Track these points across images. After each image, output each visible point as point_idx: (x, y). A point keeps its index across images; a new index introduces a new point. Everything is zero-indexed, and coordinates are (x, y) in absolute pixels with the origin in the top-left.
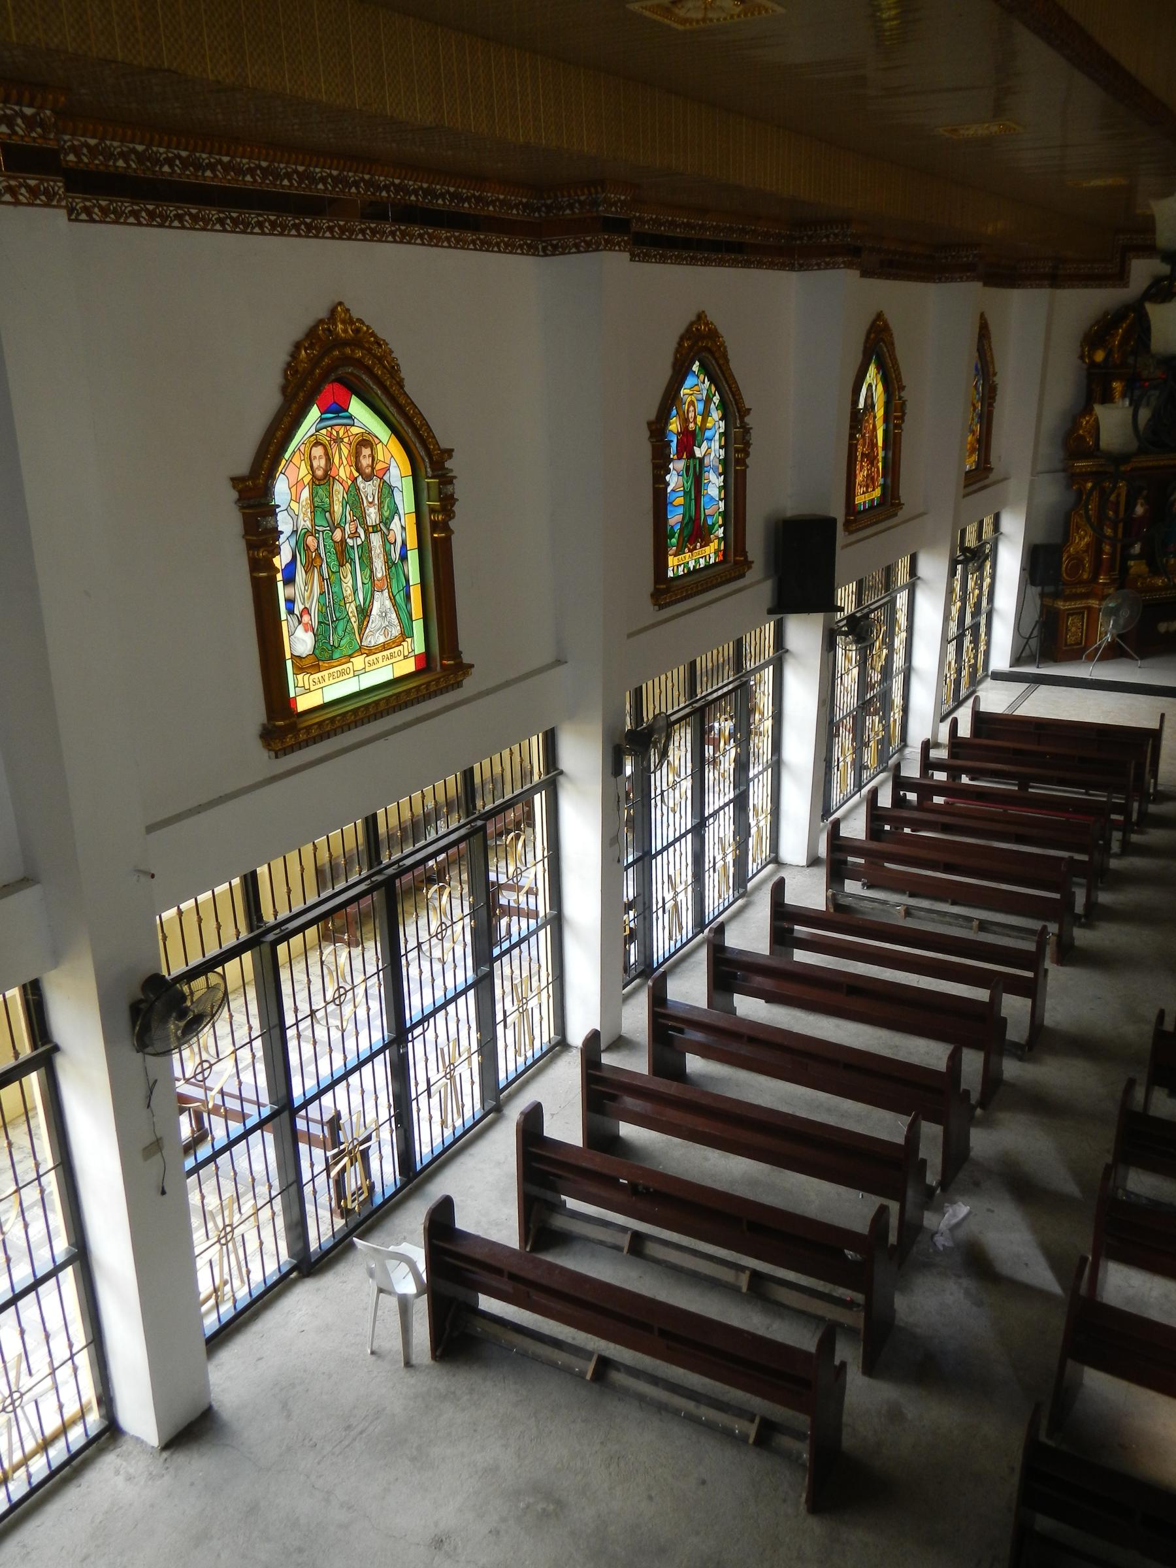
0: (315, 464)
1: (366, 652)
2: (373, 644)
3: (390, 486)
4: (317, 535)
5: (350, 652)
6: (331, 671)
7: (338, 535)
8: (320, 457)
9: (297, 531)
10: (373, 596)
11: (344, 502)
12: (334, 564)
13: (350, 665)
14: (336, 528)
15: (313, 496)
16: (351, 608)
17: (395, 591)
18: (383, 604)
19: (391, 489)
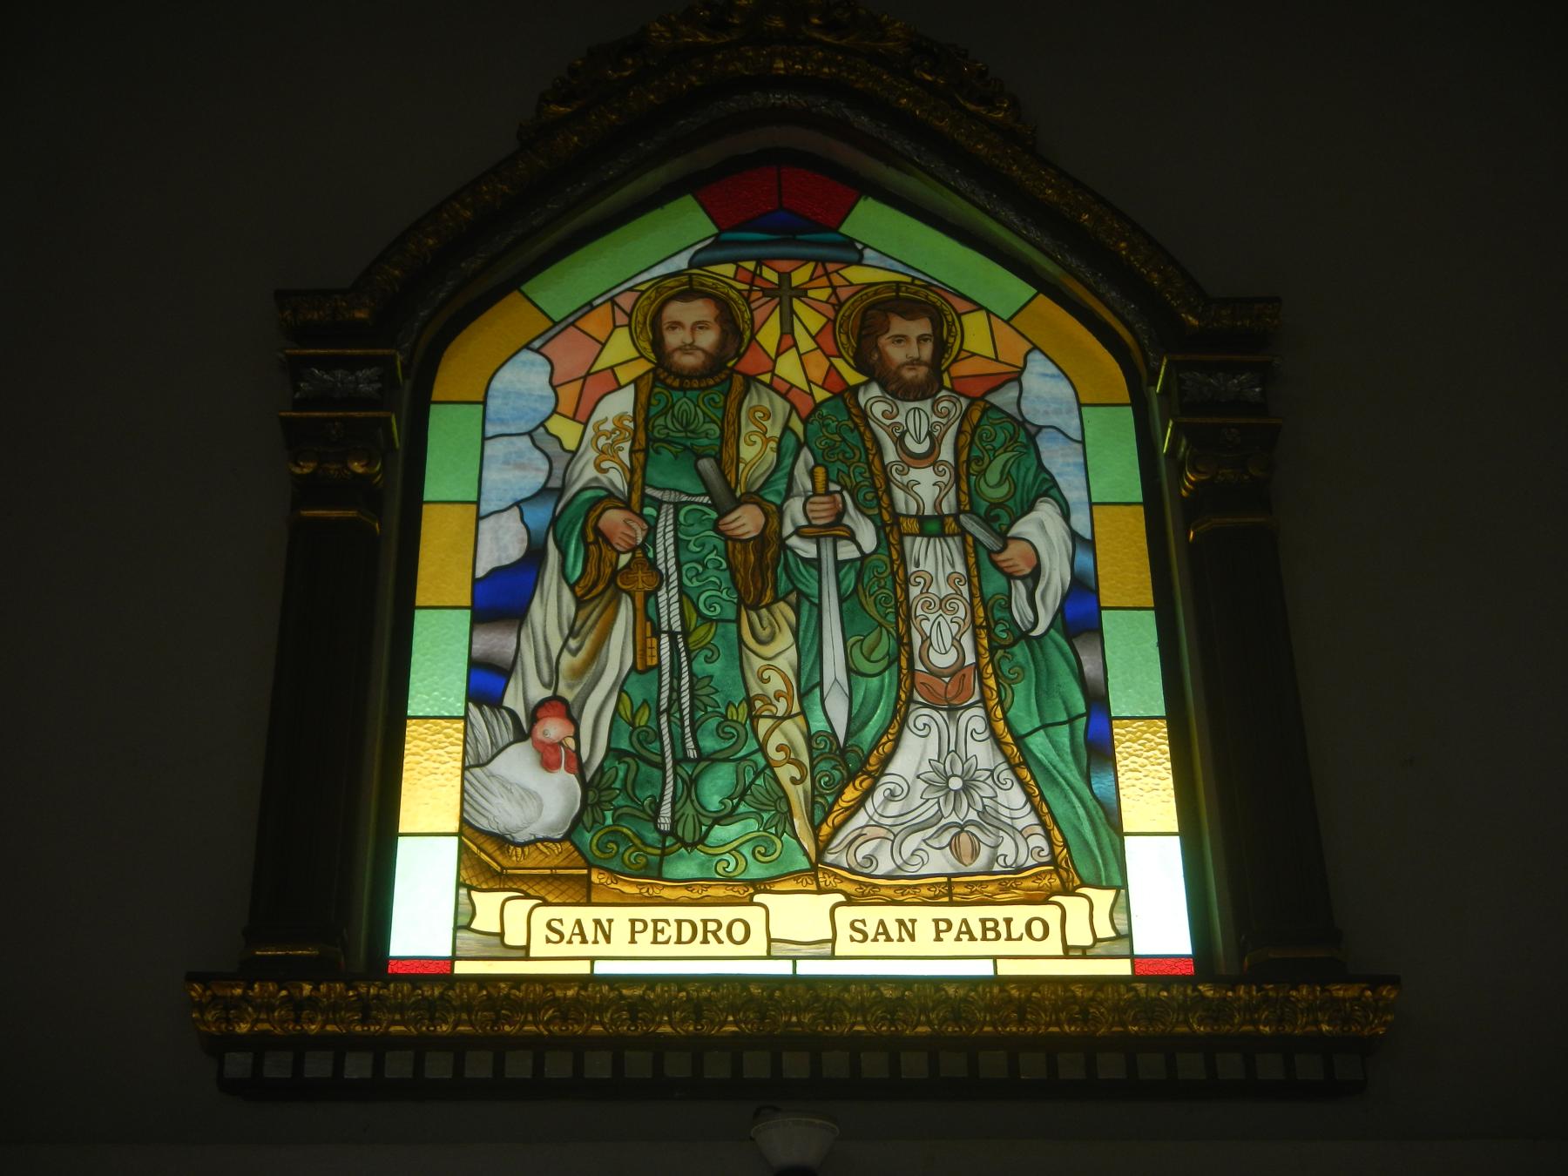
0: (673, 339)
1: (850, 888)
2: (885, 865)
3: (1021, 423)
4: (649, 511)
5: (756, 871)
6: (649, 913)
7: (747, 521)
8: (699, 326)
9: (561, 491)
10: (899, 720)
11: (790, 442)
12: (717, 598)
13: (753, 915)
14: (738, 503)
15: (644, 414)
17: (1024, 715)
19: (1025, 435)
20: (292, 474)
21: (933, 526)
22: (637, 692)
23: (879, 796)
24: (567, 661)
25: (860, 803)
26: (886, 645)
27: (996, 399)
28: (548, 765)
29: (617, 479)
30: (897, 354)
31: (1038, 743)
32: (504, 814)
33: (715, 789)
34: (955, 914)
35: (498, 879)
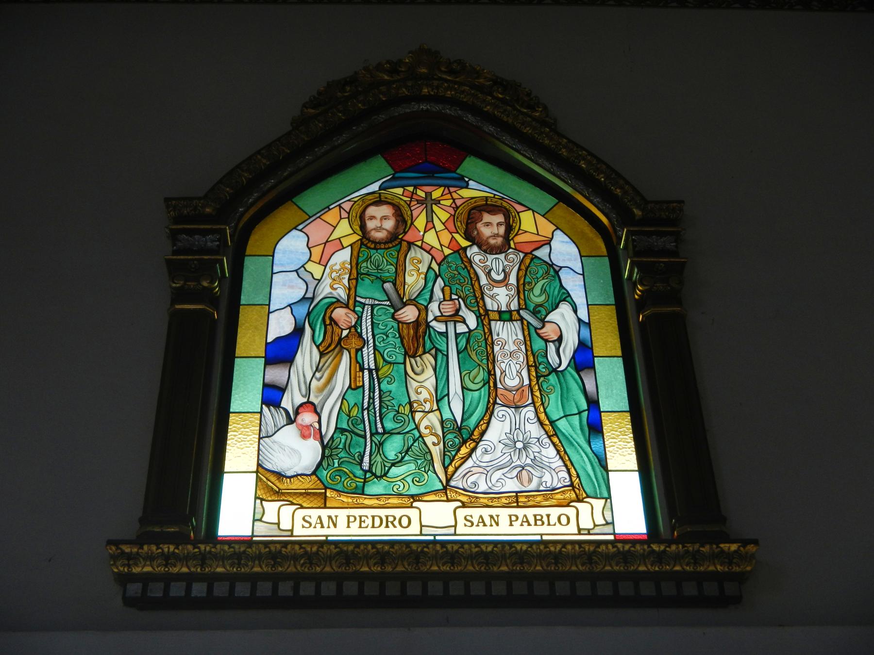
0: (370, 225)
1: (464, 499)
2: (483, 487)
3: (552, 265)
4: (358, 309)
5: (414, 490)
6: (357, 512)
8: (384, 218)
9: (313, 299)
10: (489, 412)
11: (431, 275)
12: (394, 350)
13: (413, 513)
14: (405, 305)
15: (355, 262)
16: (429, 422)
17: (555, 411)
18: (516, 427)
19: (553, 271)
20: (171, 286)
21: (505, 316)
22: (352, 398)
23: (479, 451)
24: (315, 383)
25: (469, 455)
26: (482, 375)
27: (537, 253)
28: (304, 437)
29: (342, 294)
30: (486, 232)
31: (562, 425)
32: (279, 461)
33: (393, 447)
34: (520, 512)
35: (278, 495)
